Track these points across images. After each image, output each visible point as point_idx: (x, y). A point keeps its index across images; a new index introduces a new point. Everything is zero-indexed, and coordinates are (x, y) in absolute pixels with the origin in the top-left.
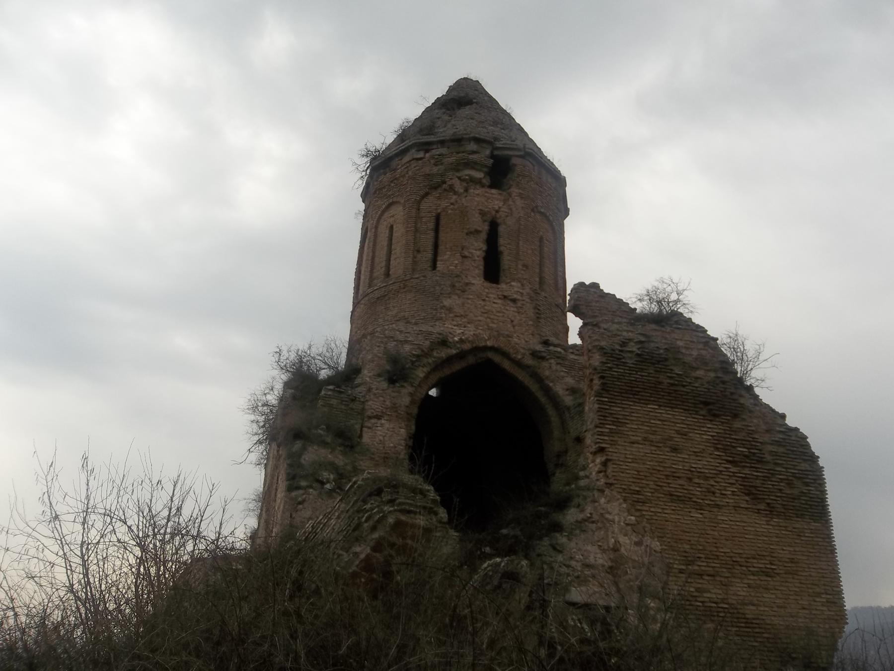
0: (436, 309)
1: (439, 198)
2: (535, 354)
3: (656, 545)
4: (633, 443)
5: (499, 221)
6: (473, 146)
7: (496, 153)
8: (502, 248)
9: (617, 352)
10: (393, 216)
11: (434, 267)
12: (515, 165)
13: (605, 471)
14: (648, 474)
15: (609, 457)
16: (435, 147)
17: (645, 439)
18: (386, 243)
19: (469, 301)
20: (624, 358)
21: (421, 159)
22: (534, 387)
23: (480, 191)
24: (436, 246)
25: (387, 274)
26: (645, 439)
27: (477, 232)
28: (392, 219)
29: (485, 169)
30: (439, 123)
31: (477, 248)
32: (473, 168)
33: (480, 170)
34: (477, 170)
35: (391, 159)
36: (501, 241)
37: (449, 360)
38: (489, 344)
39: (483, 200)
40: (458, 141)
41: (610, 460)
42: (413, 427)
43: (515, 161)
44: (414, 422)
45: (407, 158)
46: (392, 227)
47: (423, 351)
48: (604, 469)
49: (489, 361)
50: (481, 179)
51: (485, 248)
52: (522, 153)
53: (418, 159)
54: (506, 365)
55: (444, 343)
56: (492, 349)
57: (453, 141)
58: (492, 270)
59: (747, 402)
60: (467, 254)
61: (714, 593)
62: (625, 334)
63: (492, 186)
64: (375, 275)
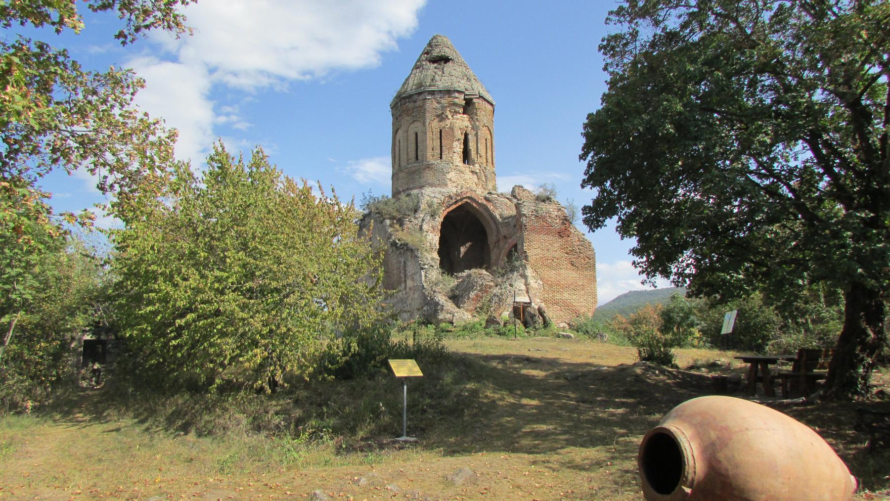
2: (486, 199)
3: (541, 283)
6: (457, 95)
11: (441, 158)
18: (414, 141)
22: (485, 214)
23: (459, 116)
30: (437, 78)
31: (458, 147)
39: (461, 121)
40: (449, 92)
43: (475, 101)
45: (422, 97)
46: (416, 134)
49: (467, 202)
55: (450, 197)
59: (572, 231)
61: (558, 296)
63: (464, 113)
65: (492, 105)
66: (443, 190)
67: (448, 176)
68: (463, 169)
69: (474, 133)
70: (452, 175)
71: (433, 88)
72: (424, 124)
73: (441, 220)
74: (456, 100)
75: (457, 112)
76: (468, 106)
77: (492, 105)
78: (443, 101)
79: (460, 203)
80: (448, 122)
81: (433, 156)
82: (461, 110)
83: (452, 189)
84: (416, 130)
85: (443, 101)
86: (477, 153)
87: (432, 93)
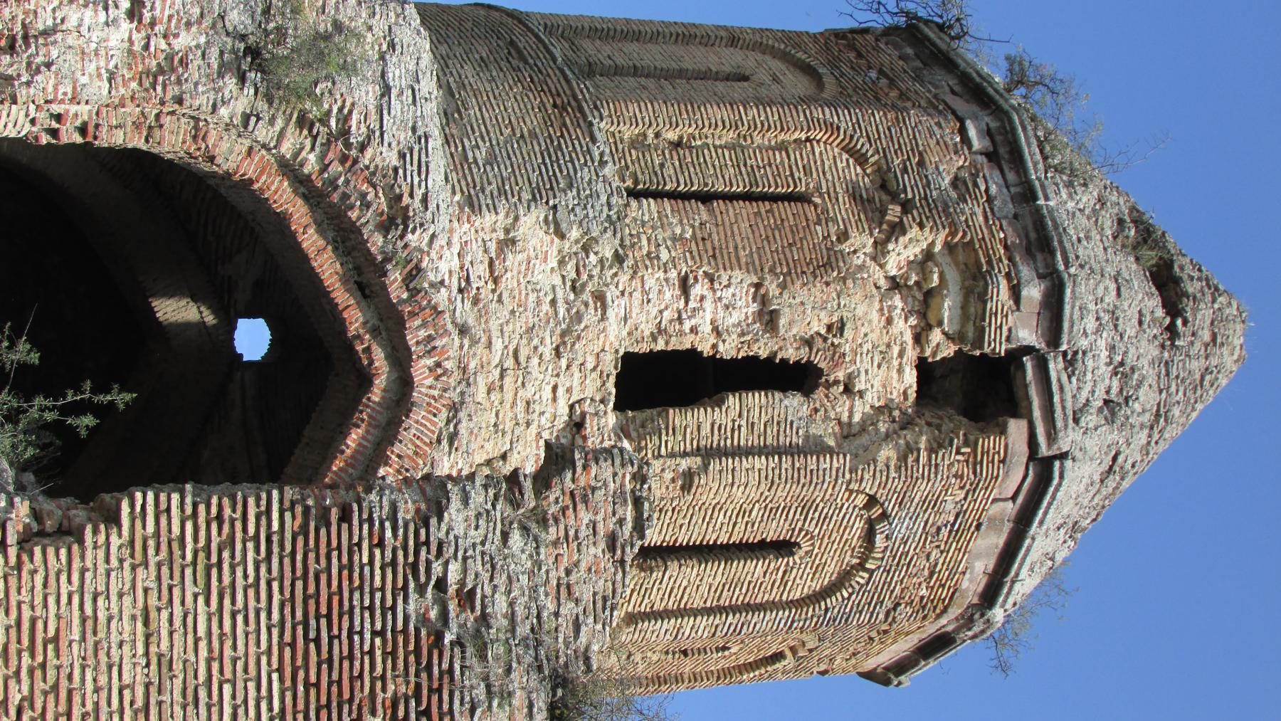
0: (502, 192)
1: (855, 195)
4: (146, 623)
5: (820, 393)
6: (1033, 292)
7: (1028, 362)
8: (732, 401)
9: (437, 568)
10: (776, 79)
11: (634, 194)
12: (1003, 431)
13: (42, 534)
14: (51, 674)
15: (89, 530)
16: (1011, 176)
17: (165, 663)
18: (688, 64)
19: (546, 307)
20: (421, 590)
21: (966, 140)
23: (903, 328)
24: (706, 198)
25: (590, 71)
26: (165, 663)
27: (769, 319)
28: (768, 80)
29: (971, 333)
31: (718, 319)
32: (967, 293)
33: (965, 317)
34: (964, 307)
35: (948, 63)
36: (756, 399)
37: (345, 238)
38: (421, 369)
40: (1040, 242)
41: (81, 542)
42: (119, 139)
43: (1017, 428)
44: (138, 142)
45: (960, 105)
47: (362, 148)
48: (49, 525)
49: (365, 379)
50: (940, 324)
51: (728, 350)
52: (1044, 451)
53: (963, 131)
54: (354, 439)
55: (397, 219)
56: (404, 383)
57: (1039, 220)
58: (659, 381)
60: (697, 291)
62: (501, 604)
63: (923, 367)
64: (586, 44)
65: (990, 595)
66: (438, 160)
67: (531, 224)
68: (585, 350)
69: (826, 432)
70: (540, 256)
71: (1031, 153)
72: (807, 101)
73: (229, 155)
74: (1002, 292)
75: (925, 307)
76: (975, 391)
77: (990, 595)
78: (974, 212)
79: (355, 318)
80: (861, 242)
81: (638, 143)
82: (940, 346)
83: (448, 245)
84: (762, 76)
85: (974, 212)
86: (708, 454)
87: (1003, 151)
